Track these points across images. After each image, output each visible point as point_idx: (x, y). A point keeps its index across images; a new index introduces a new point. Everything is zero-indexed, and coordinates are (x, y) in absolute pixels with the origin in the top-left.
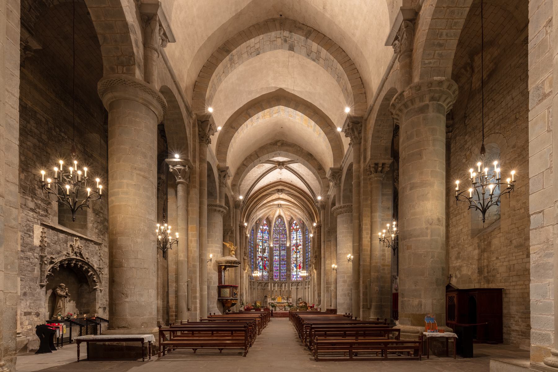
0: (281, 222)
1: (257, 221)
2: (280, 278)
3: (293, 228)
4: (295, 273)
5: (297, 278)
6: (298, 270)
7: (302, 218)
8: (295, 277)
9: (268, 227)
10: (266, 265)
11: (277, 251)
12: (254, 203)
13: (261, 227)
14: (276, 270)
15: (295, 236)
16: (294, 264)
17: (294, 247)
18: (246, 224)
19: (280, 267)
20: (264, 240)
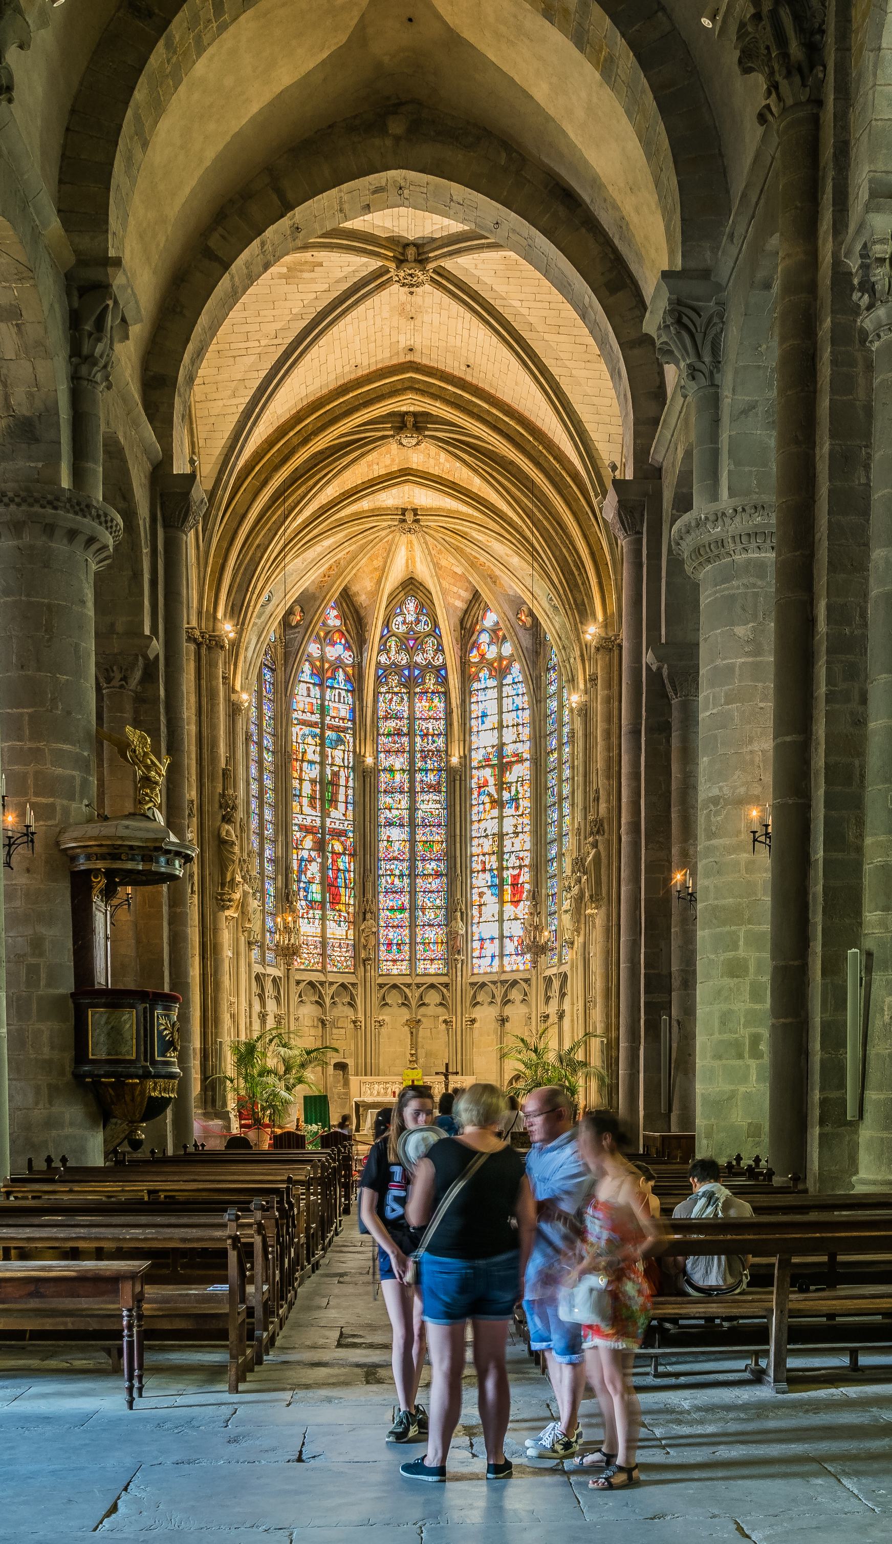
1: (290, 612)
2: (412, 960)
7: (527, 597)
11: (398, 796)
12: (274, 499)
14: (392, 909)
15: (492, 707)
18: (227, 629)
20: (331, 728)
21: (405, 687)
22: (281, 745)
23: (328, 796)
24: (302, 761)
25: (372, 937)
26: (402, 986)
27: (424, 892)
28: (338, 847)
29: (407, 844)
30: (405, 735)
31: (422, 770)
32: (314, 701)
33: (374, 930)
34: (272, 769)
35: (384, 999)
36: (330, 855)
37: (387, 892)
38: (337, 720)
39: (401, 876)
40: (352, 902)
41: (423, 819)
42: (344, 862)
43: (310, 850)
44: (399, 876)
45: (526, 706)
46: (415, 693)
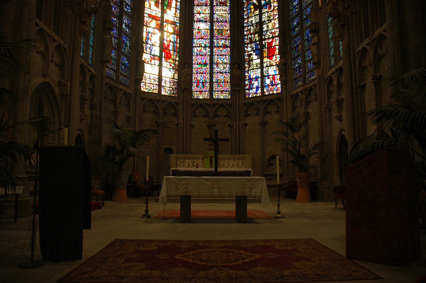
2: (211, 91)
5: (263, 87)
6: (265, 60)
8: (256, 84)
10: (171, 48)
11: (204, 8)
16: (253, 45)
19: (212, 52)
26: (205, 105)
27: (218, 55)
29: (209, 32)
33: (189, 72)
35: (194, 112)
37: (197, 55)
40: (177, 59)
41: (217, 19)
43: (154, 28)
44: (204, 47)
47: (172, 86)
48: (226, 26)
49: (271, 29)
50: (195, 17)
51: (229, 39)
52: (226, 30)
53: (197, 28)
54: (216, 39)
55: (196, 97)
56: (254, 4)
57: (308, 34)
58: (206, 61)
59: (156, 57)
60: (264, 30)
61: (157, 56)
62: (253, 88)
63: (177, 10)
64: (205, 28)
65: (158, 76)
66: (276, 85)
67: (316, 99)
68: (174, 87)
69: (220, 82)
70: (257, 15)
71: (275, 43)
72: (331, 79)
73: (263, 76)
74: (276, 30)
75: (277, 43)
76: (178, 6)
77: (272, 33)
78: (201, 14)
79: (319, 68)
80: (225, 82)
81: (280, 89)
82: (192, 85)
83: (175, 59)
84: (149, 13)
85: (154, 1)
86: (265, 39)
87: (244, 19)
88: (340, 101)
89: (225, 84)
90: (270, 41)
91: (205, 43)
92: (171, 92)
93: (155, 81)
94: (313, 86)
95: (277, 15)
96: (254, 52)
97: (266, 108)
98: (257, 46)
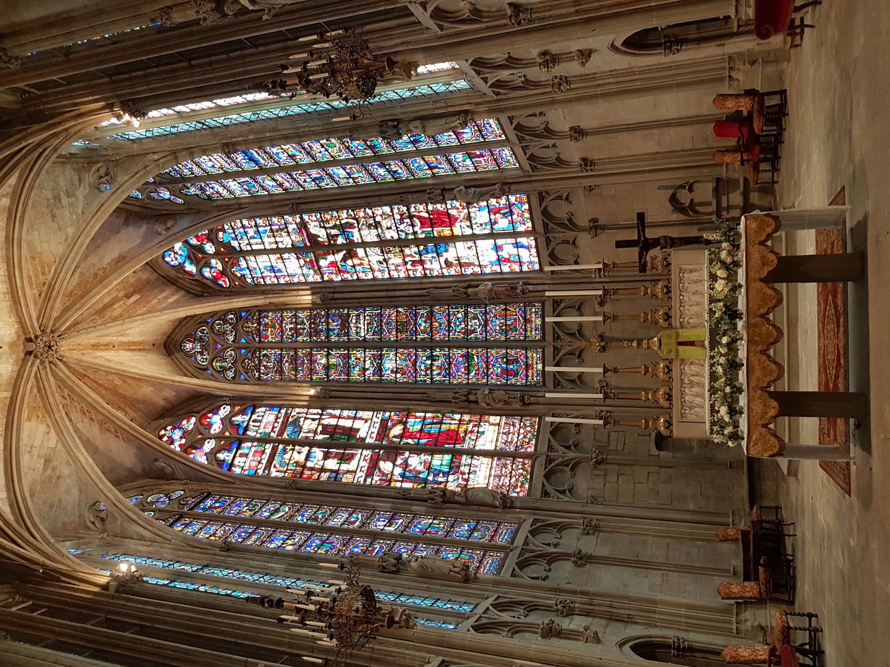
0: (201, 340)
2: (526, 345)
3: (223, 273)
4: (486, 246)
5: (515, 234)
6: (457, 231)
9: (215, 411)
10: (434, 429)
13: (209, 446)
14: (468, 371)
15: (263, 261)
16: (427, 257)
17: (323, 263)
19: (442, 345)
20: (281, 433)
21: (254, 353)
22: (279, 492)
23: (343, 439)
24: (304, 467)
25: (496, 394)
27: (449, 331)
28: (397, 430)
30: (296, 353)
31: (328, 333)
32: (254, 449)
33: (487, 392)
34: (298, 506)
36: (405, 441)
37: (450, 374)
38: (276, 425)
39: (432, 358)
40: (458, 417)
42: (414, 424)
43: (394, 464)
45: (253, 223)
46: (260, 340)
47: (516, 429)
48: (389, 316)
49: (393, 221)
50: (371, 378)
51: (415, 310)
52: (397, 316)
53: (394, 375)
54: (416, 336)
55: (538, 378)
56: (344, 259)
57: (404, 143)
58: (462, 356)
59: (454, 462)
60: (396, 236)
61: (451, 460)
62: (518, 255)
63: (358, 416)
64: (394, 358)
65: (496, 458)
66: (510, 205)
67: (541, 114)
68: (517, 425)
69: (506, 325)
70: (365, 251)
71: (422, 211)
72: (498, 84)
73: (492, 235)
74: (396, 211)
75: (421, 207)
76: (350, 414)
77: (402, 220)
78: (367, 367)
79: (473, 113)
80: (506, 316)
81: (518, 196)
82: (511, 385)
83: (458, 422)
84: (364, 475)
85: (340, 463)
86: (415, 233)
87: (374, 279)
88: (547, 57)
89: (511, 315)
90: (417, 222)
91: (424, 358)
92: (530, 431)
93: (505, 466)
94: (512, 123)
95: (364, 211)
96: (442, 256)
97: (562, 225)
98: (430, 251)
